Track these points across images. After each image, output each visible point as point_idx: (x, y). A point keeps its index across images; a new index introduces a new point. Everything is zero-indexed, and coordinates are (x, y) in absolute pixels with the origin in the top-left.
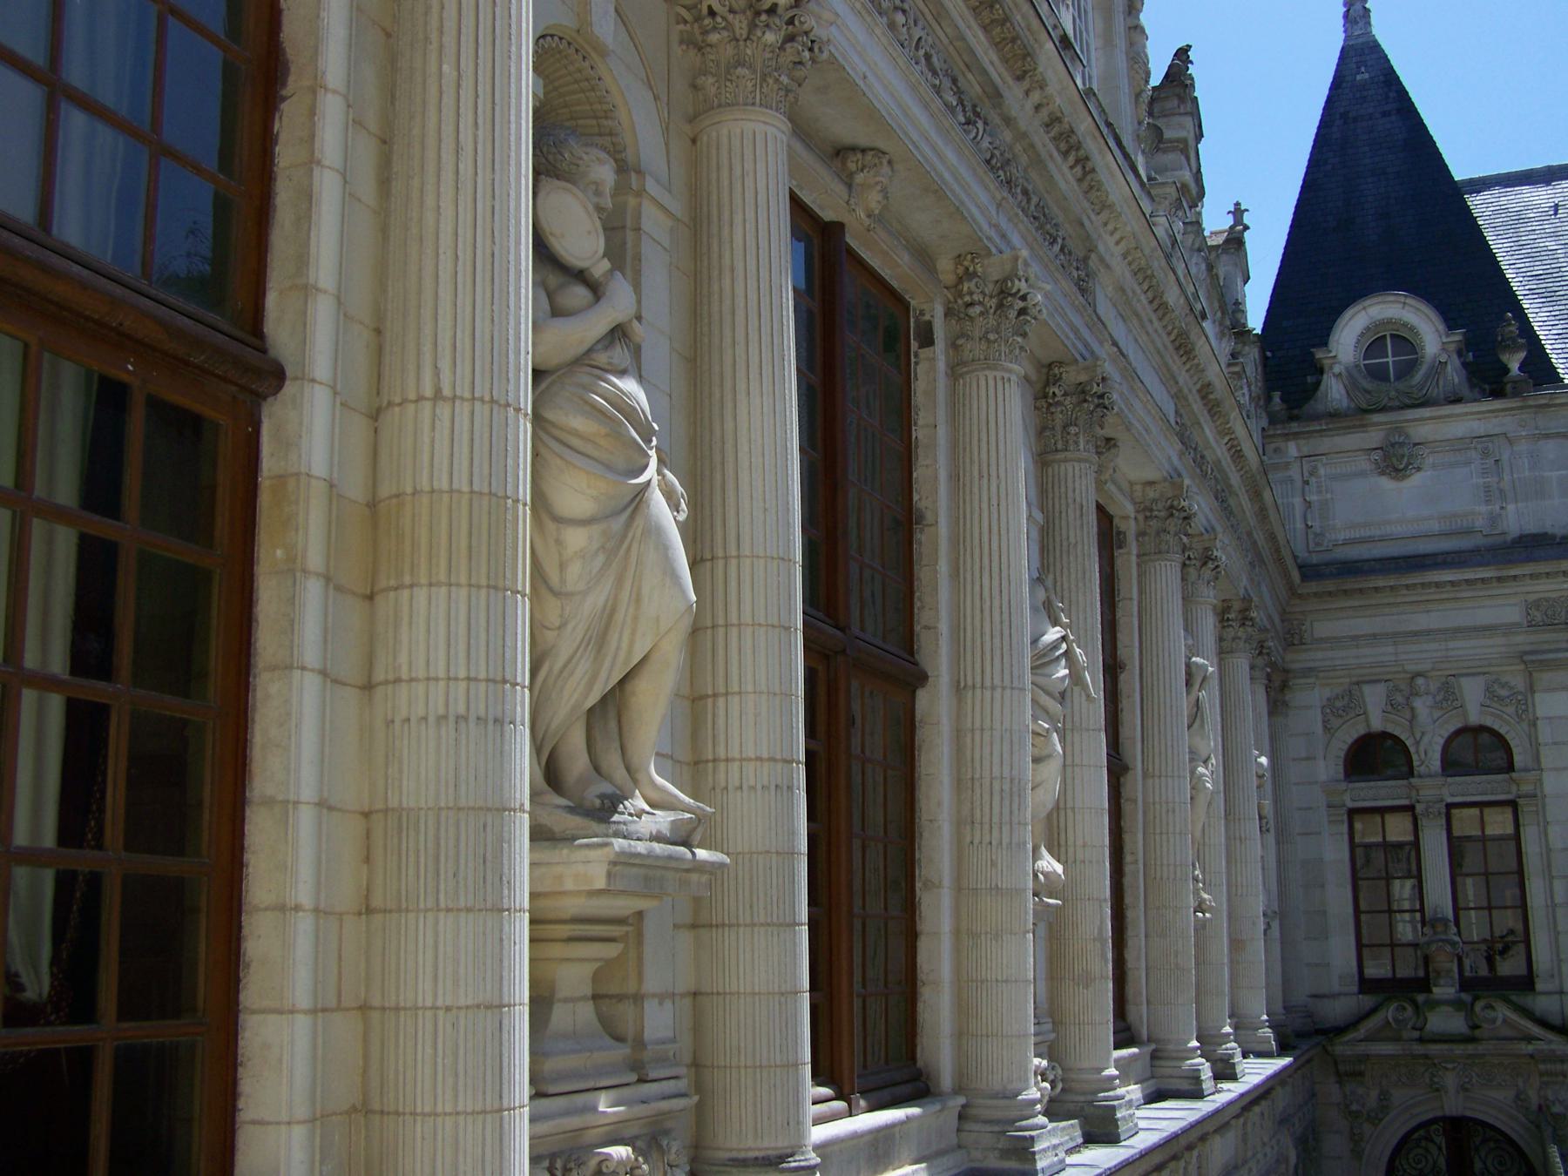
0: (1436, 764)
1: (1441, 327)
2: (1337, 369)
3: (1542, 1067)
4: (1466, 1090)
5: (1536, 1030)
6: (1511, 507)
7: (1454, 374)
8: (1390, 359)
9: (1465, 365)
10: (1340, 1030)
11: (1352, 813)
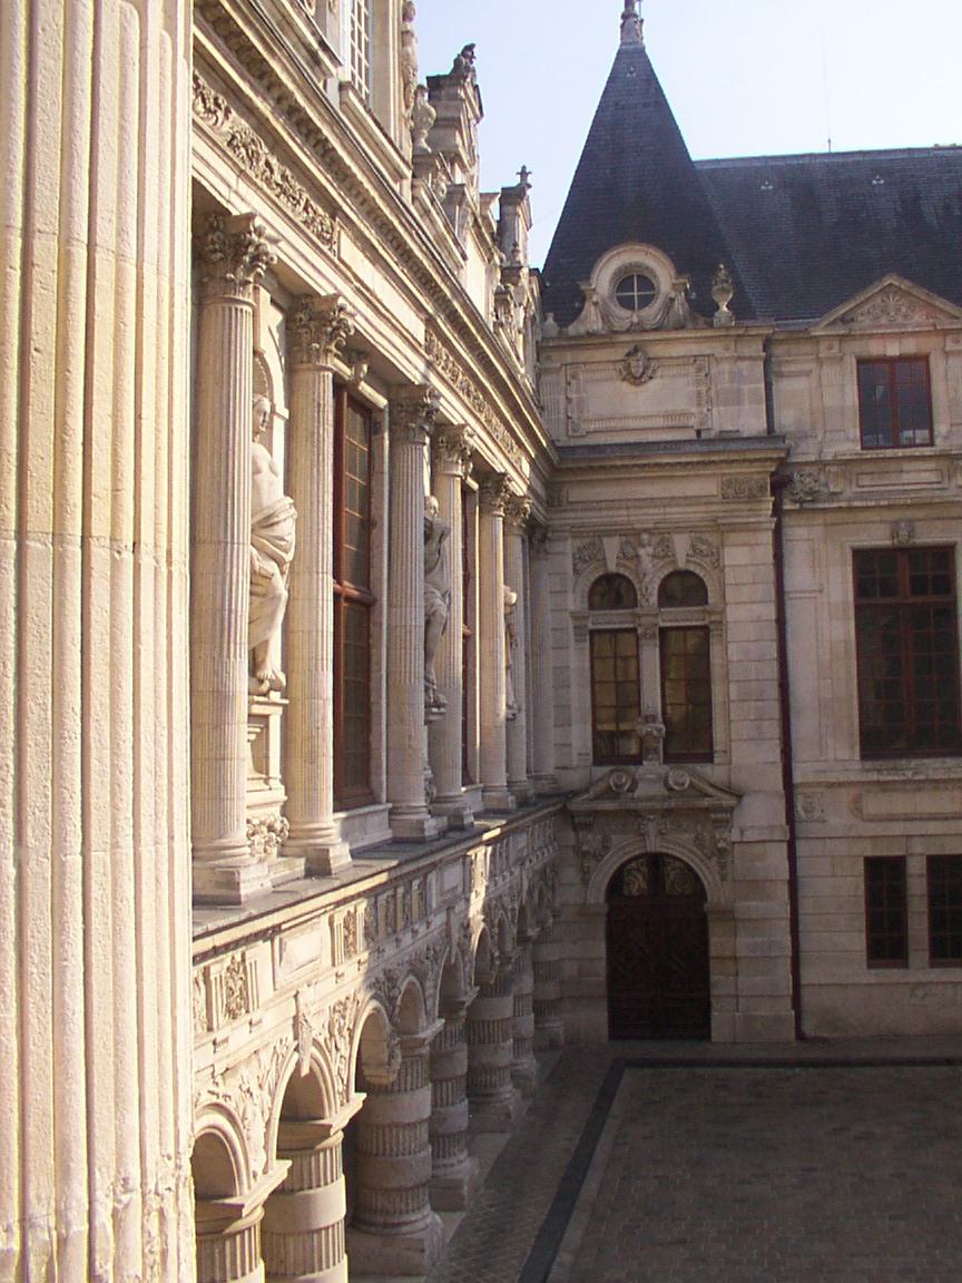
0: (654, 599)
1: (673, 272)
2: (595, 299)
3: (713, 816)
4: (662, 834)
5: (711, 790)
6: (715, 411)
7: (680, 308)
8: (636, 294)
9: (688, 301)
11: (592, 633)
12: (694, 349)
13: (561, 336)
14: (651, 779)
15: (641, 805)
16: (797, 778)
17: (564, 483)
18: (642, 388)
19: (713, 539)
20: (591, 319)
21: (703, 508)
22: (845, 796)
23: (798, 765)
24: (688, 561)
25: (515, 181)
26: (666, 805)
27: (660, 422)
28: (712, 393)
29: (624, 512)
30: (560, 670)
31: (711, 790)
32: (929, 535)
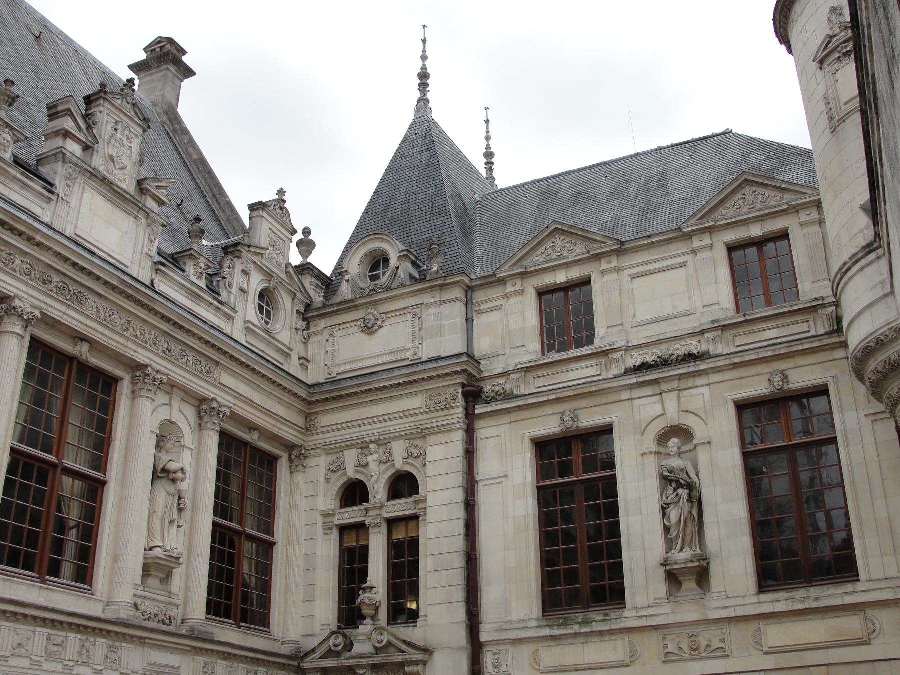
2: (347, 277)
5: (404, 647)
6: (424, 344)
10: (307, 655)
11: (343, 529)
12: (412, 301)
13: (325, 306)
14: (365, 639)
15: (354, 662)
16: (483, 638)
17: (317, 413)
18: (373, 337)
19: (418, 442)
20: (345, 291)
21: (412, 419)
22: (526, 651)
23: (459, 620)
24: (405, 463)
25: (269, 196)
26: (371, 661)
27: (387, 359)
28: (423, 331)
29: (358, 430)
30: (310, 557)
31: (404, 647)
32: (590, 419)
